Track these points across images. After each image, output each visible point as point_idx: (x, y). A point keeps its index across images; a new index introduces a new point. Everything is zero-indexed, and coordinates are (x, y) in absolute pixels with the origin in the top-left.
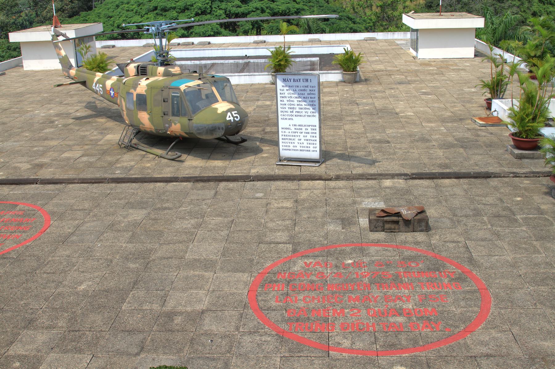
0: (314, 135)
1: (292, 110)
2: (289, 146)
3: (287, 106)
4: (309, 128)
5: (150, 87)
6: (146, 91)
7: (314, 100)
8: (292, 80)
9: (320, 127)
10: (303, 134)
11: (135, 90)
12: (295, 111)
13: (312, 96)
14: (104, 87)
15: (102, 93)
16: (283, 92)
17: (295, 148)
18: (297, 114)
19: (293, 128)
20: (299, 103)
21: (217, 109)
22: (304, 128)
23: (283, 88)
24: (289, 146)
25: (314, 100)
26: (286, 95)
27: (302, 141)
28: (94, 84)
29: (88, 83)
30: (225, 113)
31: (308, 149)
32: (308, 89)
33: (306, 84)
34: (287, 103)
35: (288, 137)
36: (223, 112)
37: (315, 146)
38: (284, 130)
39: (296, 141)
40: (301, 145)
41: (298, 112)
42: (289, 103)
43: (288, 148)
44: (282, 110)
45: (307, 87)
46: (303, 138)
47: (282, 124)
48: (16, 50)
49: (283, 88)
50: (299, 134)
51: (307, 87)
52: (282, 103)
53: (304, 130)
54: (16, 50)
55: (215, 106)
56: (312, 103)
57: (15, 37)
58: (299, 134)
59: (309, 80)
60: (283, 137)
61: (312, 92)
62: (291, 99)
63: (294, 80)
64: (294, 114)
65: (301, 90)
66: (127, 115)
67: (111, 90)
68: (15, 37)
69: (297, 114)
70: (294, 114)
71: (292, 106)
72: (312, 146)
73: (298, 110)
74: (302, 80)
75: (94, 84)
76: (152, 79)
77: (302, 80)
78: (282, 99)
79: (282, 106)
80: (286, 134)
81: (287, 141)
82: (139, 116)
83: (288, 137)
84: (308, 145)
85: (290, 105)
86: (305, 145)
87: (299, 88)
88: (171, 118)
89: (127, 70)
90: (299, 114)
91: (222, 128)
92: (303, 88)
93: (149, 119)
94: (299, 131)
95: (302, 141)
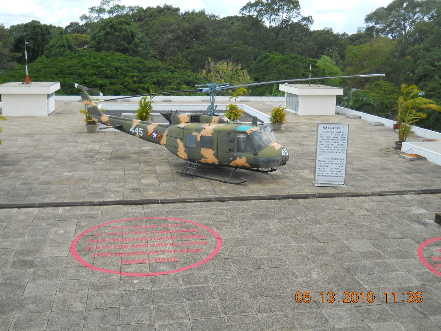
0: (342, 165)
1: (327, 148)
2: (323, 173)
3: (324, 146)
4: (339, 161)
6: (212, 134)
7: (344, 141)
8: (330, 128)
9: (346, 160)
10: (334, 165)
12: (329, 149)
13: (343, 139)
15: (141, 135)
16: (322, 136)
17: (327, 175)
18: (331, 151)
20: (333, 143)
23: (322, 133)
24: (323, 173)
25: (344, 141)
26: (324, 138)
28: (133, 128)
31: (337, 175)
33: (340, 130)
34: (324, 143)
35: (323, 167)
36: (279, 149)
37: (342, 173)
40: (332, 173)
41: (332, 150)
42: (326, 143)
43: (322, 175)
44: (320, 148)
45: (340, 132)
46: (333, 167)
47: (319, 158)
49: (322, 133)
50: (331, 165)
51: (340, 132)
52: (321, 143)
53: (335, 162)
56: (342, 144)
58: (331, 165)
59: (342, 128)
60: (319, 167)
61: (343, 136)
62: (328, 141)
64: (329, 151)
65: (336, 135)
67: (153, 132)
69: (331, 151)
70: (329, 151)
71: (328, 146)
72: (339, 173)
73: (332, 148)
74: (336, 128)
75: (133, 128)
77: (336, 128)
78: (321, 141)
79: (320, 146)
80: (321, 165)
81: (322, 169)
82: (202, 152)
83: (323, 167)
84: (337, 173)
86: (335, 172)
87: (334, 133)
90: (332, 151)
91: (278, 161)
92: (336, 133)
93: (214, 155)
94: (331, 163)
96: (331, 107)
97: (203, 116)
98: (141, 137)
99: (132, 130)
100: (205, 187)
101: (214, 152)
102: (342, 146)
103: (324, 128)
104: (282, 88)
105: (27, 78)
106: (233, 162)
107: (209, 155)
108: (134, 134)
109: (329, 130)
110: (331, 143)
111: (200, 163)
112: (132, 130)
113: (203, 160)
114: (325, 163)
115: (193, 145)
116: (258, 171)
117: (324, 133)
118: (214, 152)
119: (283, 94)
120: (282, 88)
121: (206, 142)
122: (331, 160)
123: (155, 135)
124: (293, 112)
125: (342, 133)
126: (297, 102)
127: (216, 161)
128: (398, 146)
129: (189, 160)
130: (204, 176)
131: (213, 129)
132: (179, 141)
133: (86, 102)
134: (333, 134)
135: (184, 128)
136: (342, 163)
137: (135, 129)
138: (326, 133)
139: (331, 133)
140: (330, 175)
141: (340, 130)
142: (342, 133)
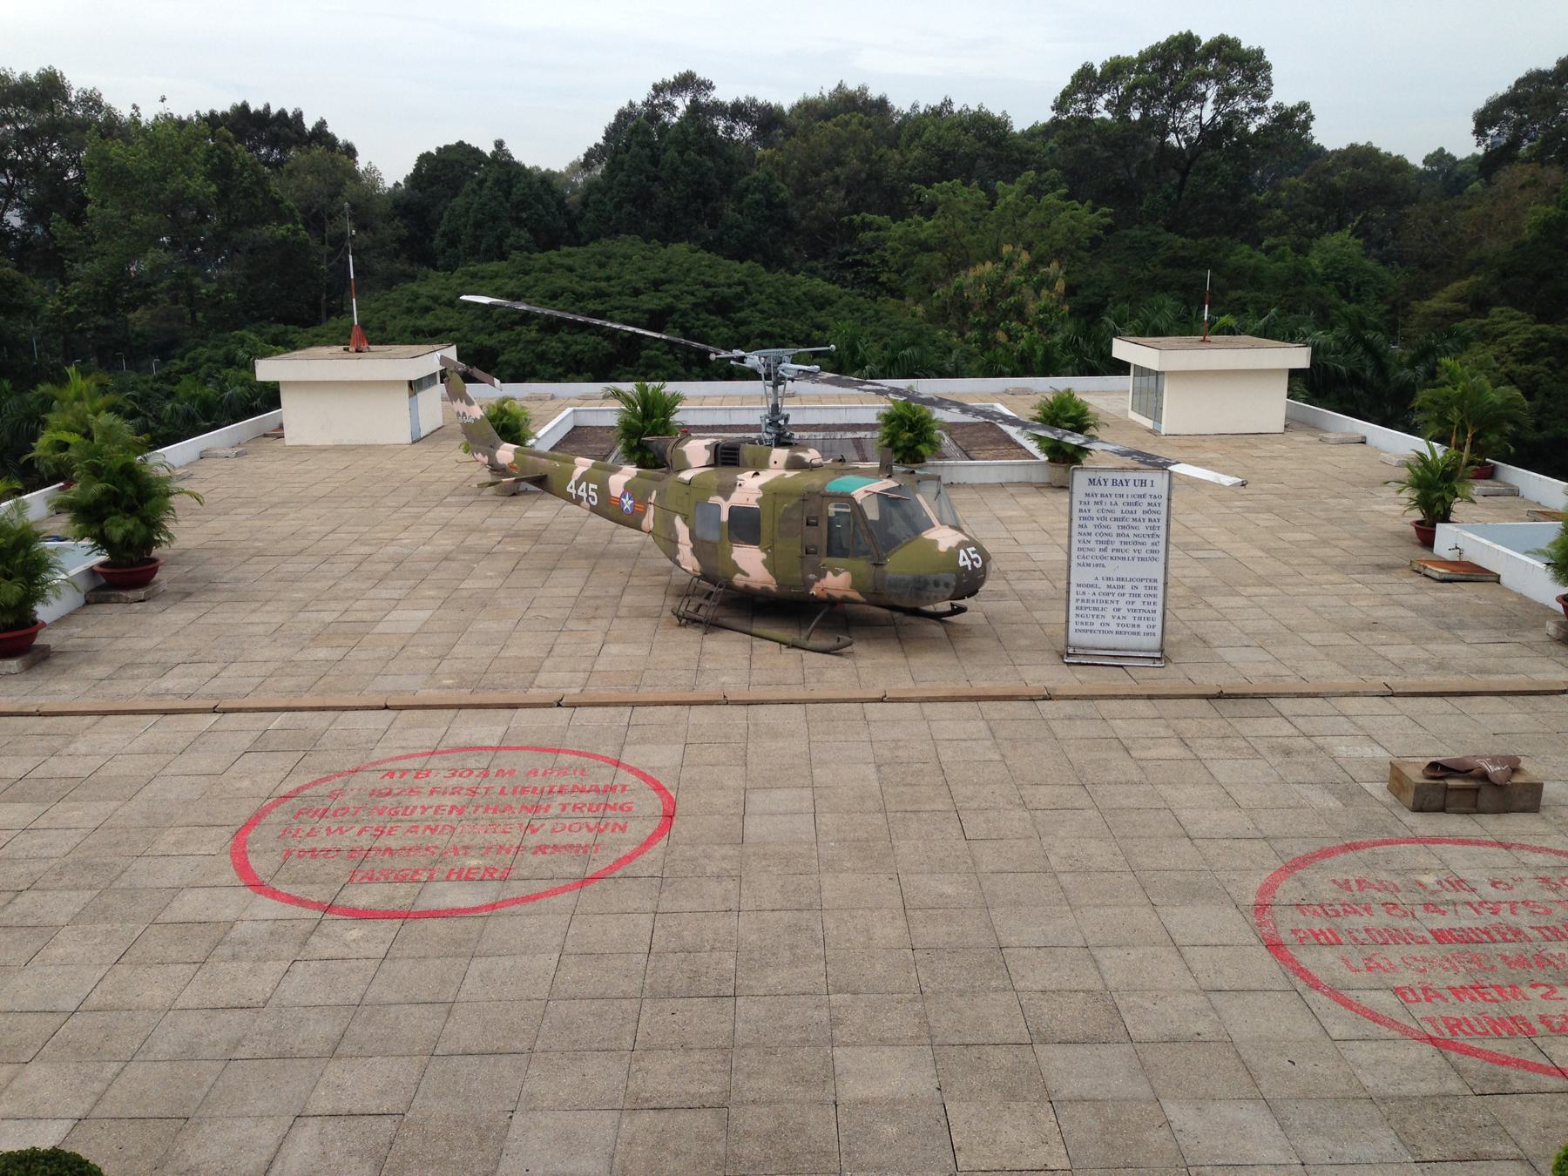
0: (1151, 600)
3: (1093, 538)
4: (1141, 585)
5: (771, 493)
6: (758, 501)
8: (1109, 483)
10: (1127, 598)
11: (727, 498)
12: (1110, 547)
13: (1153, 516)
14: (603, 491)
19: (1103, 585)
21: (935, 543)
22: (1128, 585)
26: (1094, 514)
27: (1123, 612)
28: (572, 483)
29: (554, 480)
30: (953, 553)
32: (1145, 501)
33: (1141, 490)
34: (1093, 531)
38: (1081, 589)
39: (1109, 613)
48: (270, 397)
50: (1116, 598)
53: (1128, 590)
54: (270, 397)
55: (929, 535)
57: (267, 370)
58: (1116, 598)
60: (1080, 604)
63: (1114, 482)
64: (1109, 553)
66: (694, 551)
67: (623, 495)
68: (267, 370)
70: (1109, 553)
72: (1144, 624)
73: (1117, 545)
74: (1131, 483)
75: (572, 483)
76: (766, 477)
85: (1101, 534)
86: (1130, 620)
87: (1125, 499)
88: (826, 560)
89: (683, 454)
91: (947, 585)
92: (1131, 500)
93: (765, 563)
94: (1117, 591)
95: (1123, 612)
96: (1270, 406)
97: (746, 452)
98: (593, 509)
99: (571, 489)
100: (734, 660)
101: (764, 556)
102: (1150, 540)
103: (1092, 482)
104: (1122, 349)
105: (356, 333)
106: (817, 585)
107: (751, 565)
108: (577, 501)
109: (1109, 489)
110: (1114, 530)
111: (730, 586)
112: (571, 489)
113: (739, 580)
114: (1097, 591)
115: (712, 535)
116: (917, 613)
117: (1092, 500)
118: (764, 556)
119: (1122, 368)
120: (1122, 349)
121: (745, 525)
122: (1116, 583)
123: (627, 503)
124: (1149, 423)
125: (1148, 500)
126: (1158, 393)
127: (773, 586)
128: (1426, 536)
129: (704, 576)
130: (747, 629)
131: (762, 488)
132: (678, 521)
133: (460, 406)
134: (1120, 501)
135: (690, 482)
136: (1152, 592)
137: (578, 484)
138: (1098, 499)
139: (1113, 499)
140: (1113, 627)
141: (1141, 490)
142: (1148, 500)
